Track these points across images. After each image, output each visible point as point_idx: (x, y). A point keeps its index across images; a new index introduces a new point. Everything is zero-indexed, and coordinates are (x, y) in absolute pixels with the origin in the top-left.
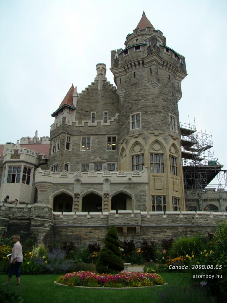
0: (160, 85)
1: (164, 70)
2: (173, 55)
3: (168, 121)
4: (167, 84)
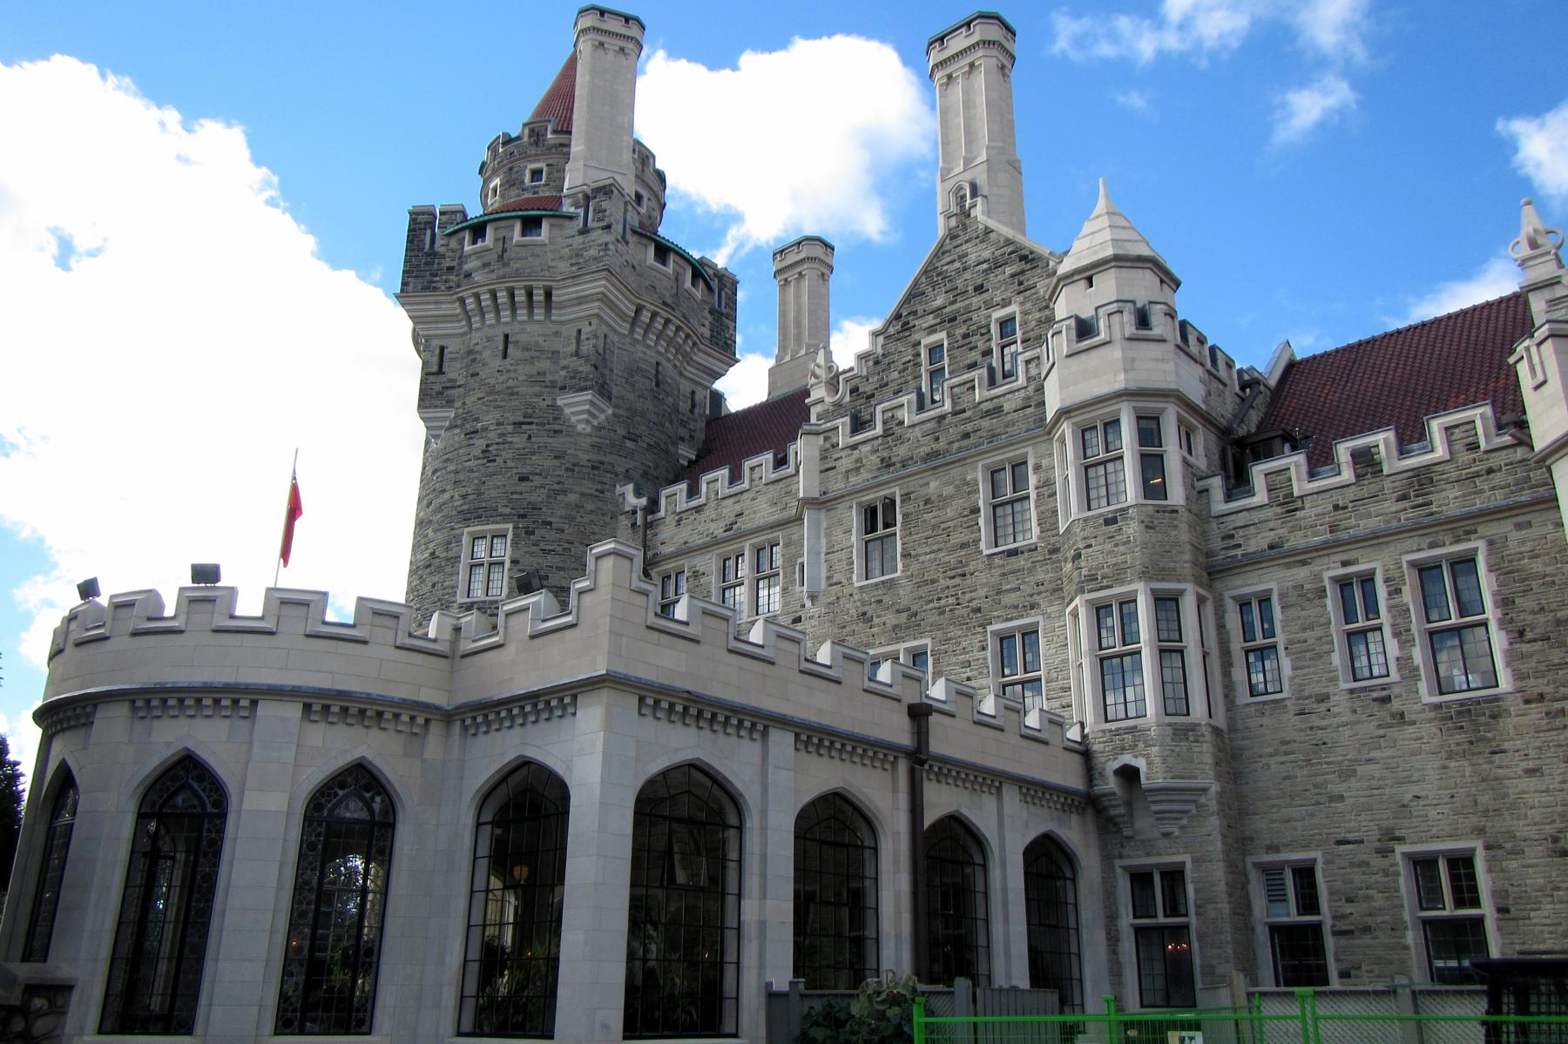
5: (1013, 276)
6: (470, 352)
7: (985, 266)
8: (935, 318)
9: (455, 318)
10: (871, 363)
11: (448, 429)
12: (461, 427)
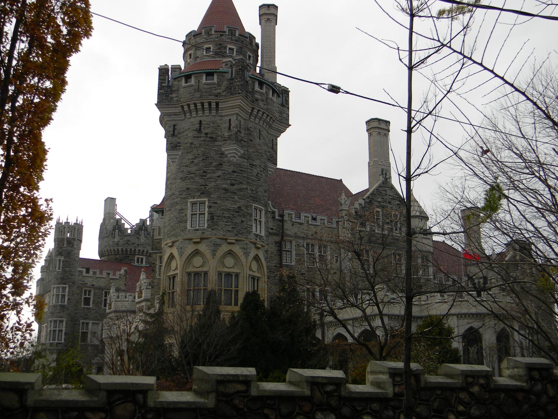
0: (180, 153)
1: (189, 118)
2: (202, 79)
3: (186, 215)
4: (192, 143)
5: (398, 204)
6: (248, 129)
7: (391, 197)
8: (379, 204)
9: (247, 112)
10: (361, 207)
11: (239, 157)
12: (248, 160)
